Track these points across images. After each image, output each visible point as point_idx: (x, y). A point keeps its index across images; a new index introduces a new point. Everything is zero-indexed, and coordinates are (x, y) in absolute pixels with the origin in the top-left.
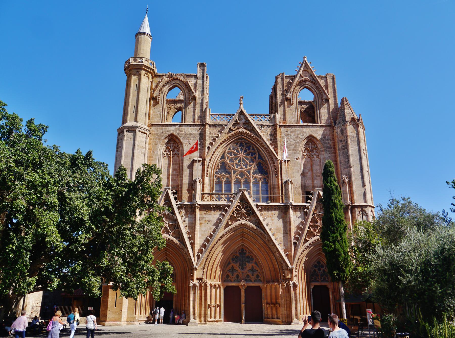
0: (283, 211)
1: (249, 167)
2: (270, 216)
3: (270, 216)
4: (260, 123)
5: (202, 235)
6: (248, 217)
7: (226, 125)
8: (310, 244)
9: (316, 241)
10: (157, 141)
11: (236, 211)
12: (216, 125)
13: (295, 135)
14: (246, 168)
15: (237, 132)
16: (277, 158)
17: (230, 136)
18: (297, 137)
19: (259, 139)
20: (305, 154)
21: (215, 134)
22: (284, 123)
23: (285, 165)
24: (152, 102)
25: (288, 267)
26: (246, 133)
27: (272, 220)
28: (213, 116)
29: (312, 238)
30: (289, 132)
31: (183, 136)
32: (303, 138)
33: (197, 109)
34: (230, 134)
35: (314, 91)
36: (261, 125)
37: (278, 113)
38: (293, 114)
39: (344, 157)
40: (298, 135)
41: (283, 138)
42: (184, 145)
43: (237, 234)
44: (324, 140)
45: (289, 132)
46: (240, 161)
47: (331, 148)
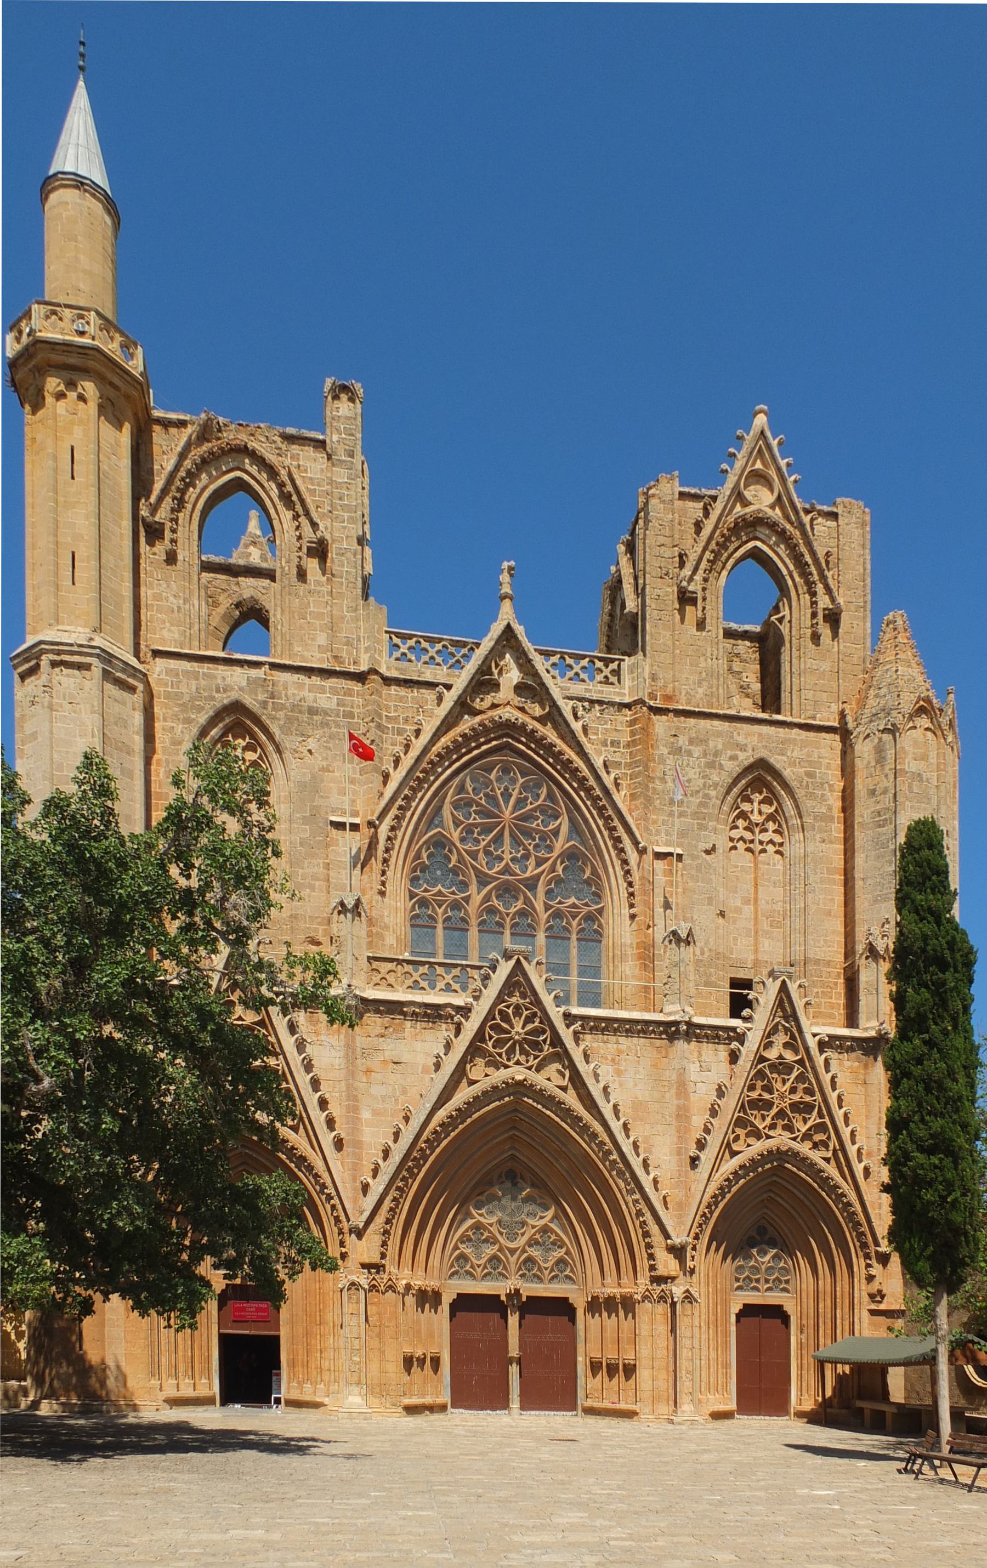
0: (658, 1042)
2: (613, 1060)
3: (613, 1060)
4: (578, 689)
5: (375, 1113)
6: (535, 1059)
7: (448, 687)
8: (742, 1167)
9: (762, 1155)
11: (492, 1033)
12: (411, 681)
13: (705, 754)
14: (525, 872)
15: (492, 720)
16: (639, 843)
17: (464, 736)
18: (711, 765)
19: (574, 757)
21: (406, 720)
25: (667, 1236)
26: (524, 725)
27: (619, 1073)
28: (396, 640)
29: (749, 1145)
30: (682, 741)
31: (281, 714)
32: (733, 768)
35: (785, 572)
36: (581, 699)
37: (645, 655)
38: (703, 665)
39: (878, 857)
40: (717, 754)
41: (662, 761)
42: (287, 755)
43: (497, 1118)
44: (807, 786)
45: (682, 741)
47: (831, 819)
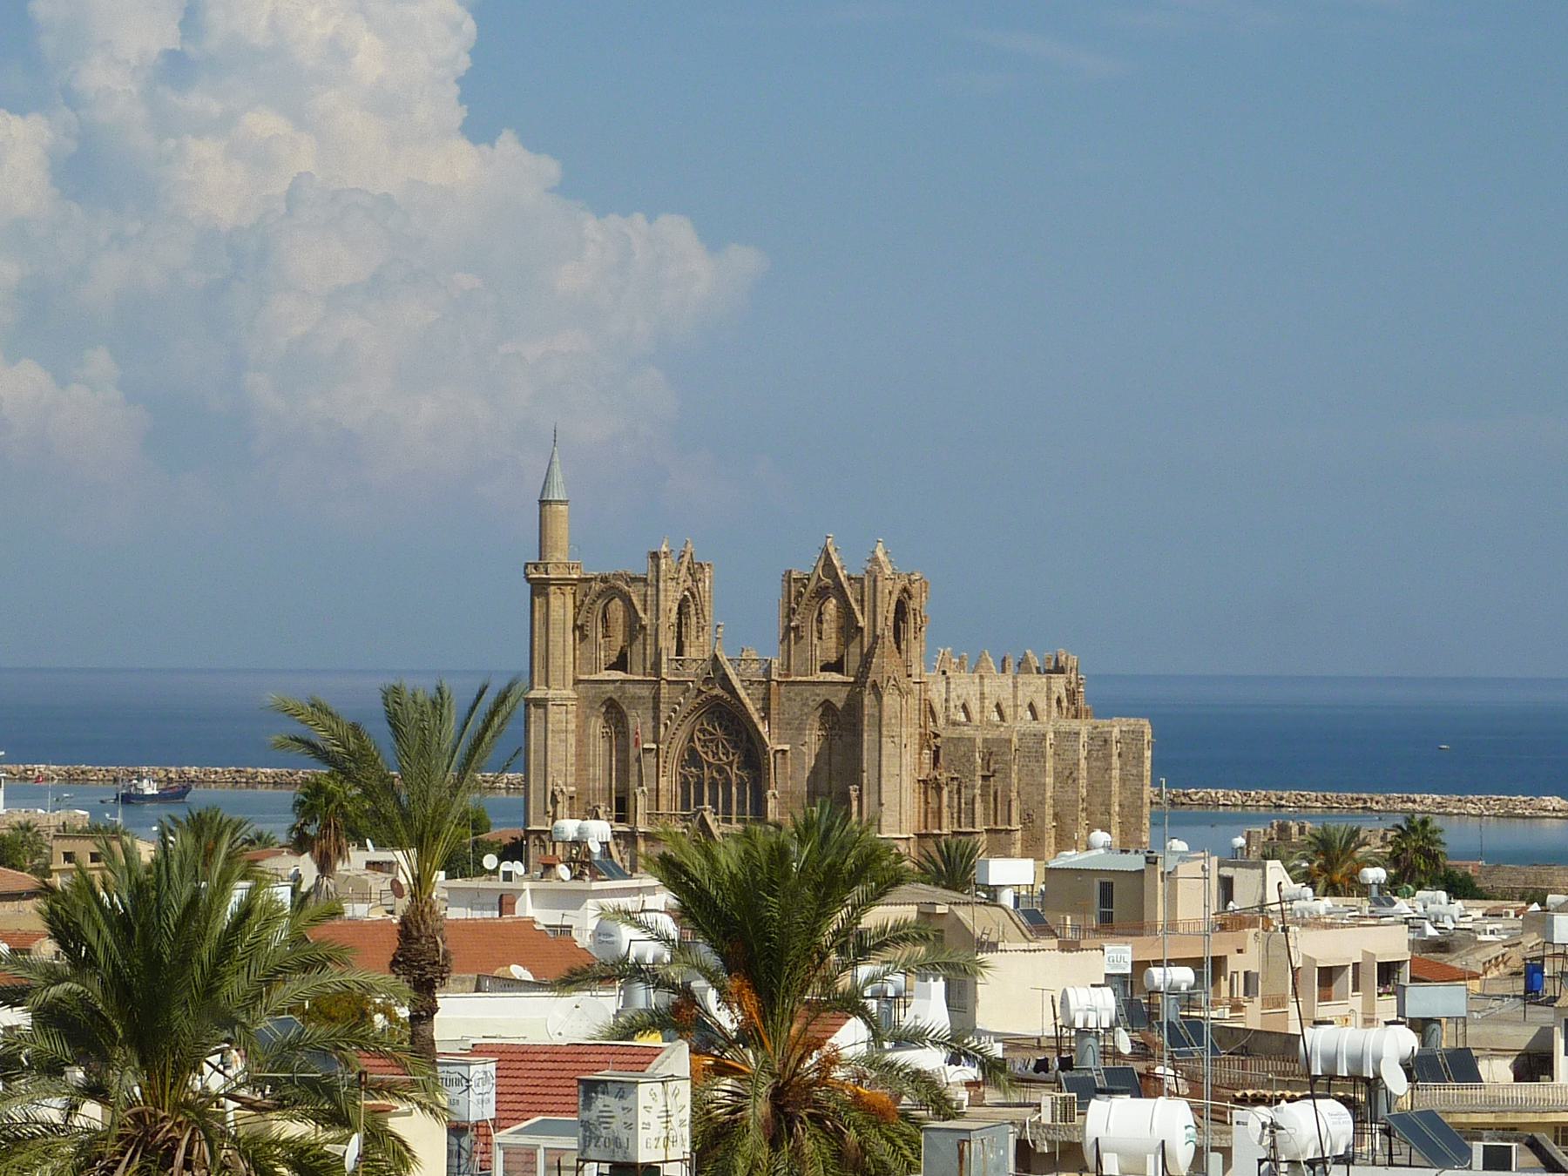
1: (731, 758)
10: (588, 711)
18: (804, 704)
20: (819, 733)
22: (787, 675)
23: (782, 758)
24: (577, 633)
33: (648, 647)
34: (699, 701)
40: (807, 699)
46: (717, 747)
